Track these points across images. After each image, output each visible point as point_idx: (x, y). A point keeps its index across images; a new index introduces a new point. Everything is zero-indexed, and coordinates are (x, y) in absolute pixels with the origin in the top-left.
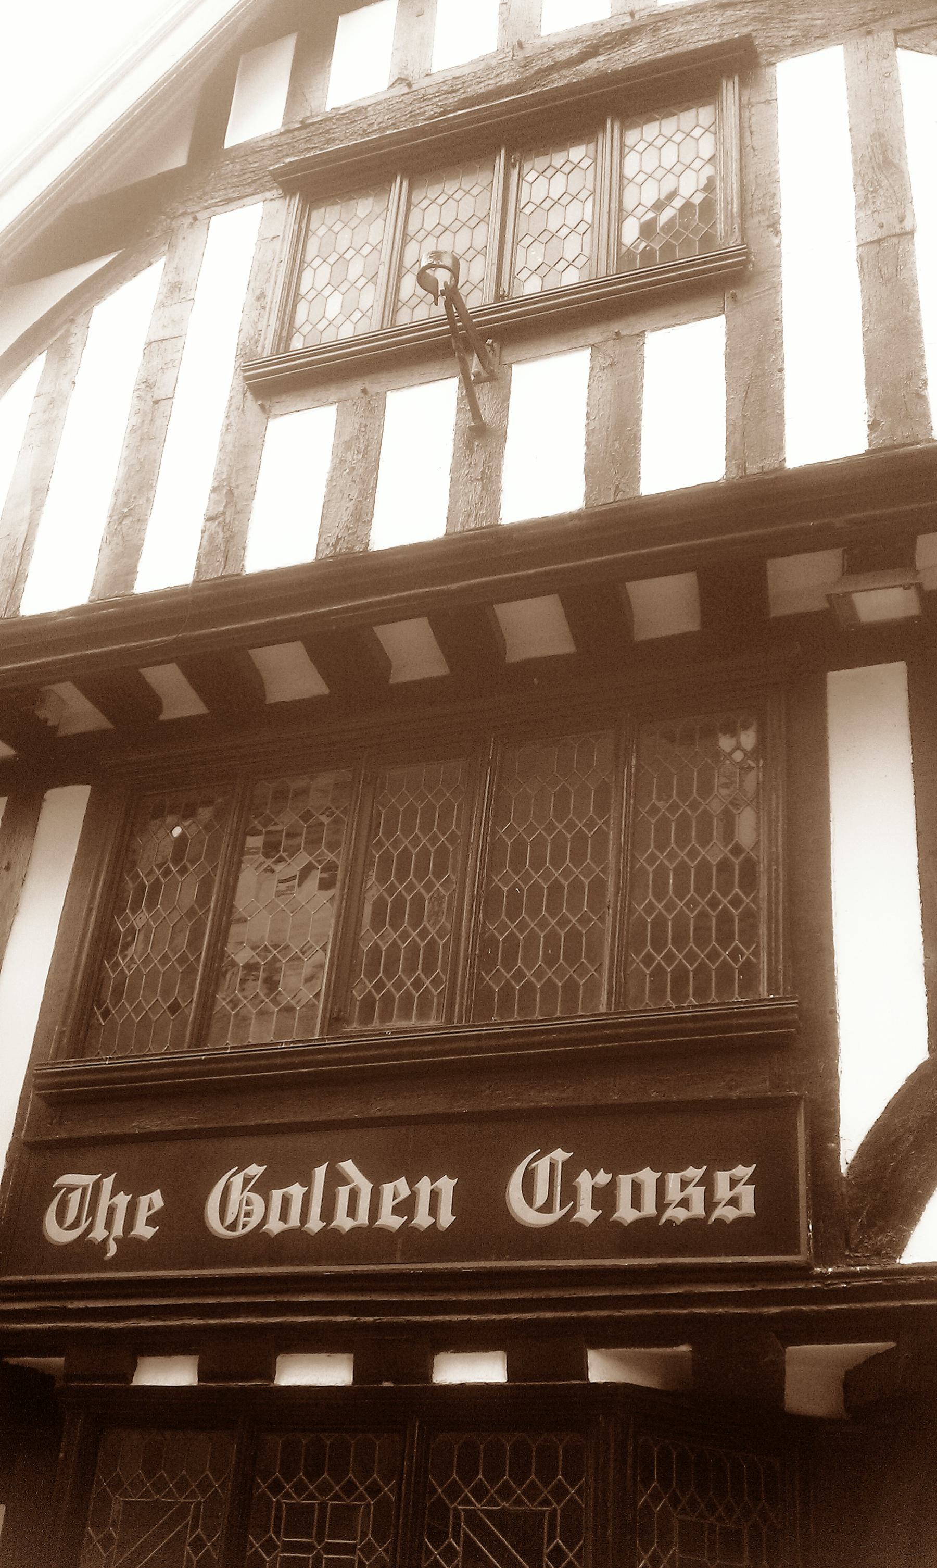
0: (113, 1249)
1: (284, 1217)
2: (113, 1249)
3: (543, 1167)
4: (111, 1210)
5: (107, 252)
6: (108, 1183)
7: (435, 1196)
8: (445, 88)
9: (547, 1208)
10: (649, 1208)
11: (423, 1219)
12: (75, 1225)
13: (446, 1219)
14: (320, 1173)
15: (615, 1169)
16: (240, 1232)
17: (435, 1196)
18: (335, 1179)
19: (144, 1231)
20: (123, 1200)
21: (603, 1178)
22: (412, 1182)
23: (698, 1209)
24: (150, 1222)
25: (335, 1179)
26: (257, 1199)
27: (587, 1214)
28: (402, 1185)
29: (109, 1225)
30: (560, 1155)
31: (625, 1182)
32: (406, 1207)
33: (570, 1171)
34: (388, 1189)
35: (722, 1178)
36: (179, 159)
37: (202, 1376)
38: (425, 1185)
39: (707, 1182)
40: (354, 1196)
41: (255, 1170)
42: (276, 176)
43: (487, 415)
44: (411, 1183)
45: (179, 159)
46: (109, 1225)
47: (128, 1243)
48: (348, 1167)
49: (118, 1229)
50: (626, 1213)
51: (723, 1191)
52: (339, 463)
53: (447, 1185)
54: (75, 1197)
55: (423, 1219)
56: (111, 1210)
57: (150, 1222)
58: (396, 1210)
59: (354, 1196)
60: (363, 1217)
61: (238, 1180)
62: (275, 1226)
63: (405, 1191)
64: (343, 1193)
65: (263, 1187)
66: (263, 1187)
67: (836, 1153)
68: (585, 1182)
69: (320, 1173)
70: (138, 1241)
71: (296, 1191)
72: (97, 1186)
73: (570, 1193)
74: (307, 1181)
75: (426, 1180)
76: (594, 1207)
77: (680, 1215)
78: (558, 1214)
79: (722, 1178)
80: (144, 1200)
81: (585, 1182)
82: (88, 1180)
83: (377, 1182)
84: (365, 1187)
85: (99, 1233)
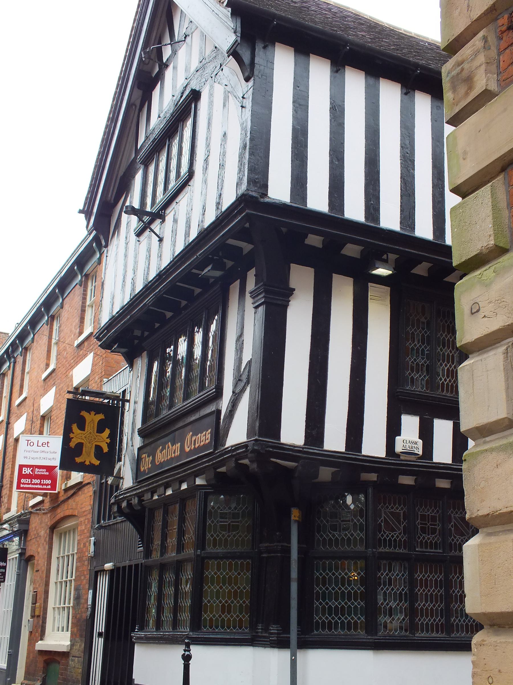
11: (176, 454)
13: (179, 453)
15: (196, 436)
20: (148, 458)
25: (168, 447)
26: (161, 454)
30: (191, 433)
31: (197, 437)
37: (158, 497)
38: (177, 446)
47: (148, 468)
50: (197, 446)
53: (179, 444)
55: (176, 454)
62: (162, 460)
74: (166, 449)
76: (194, 445)
78: (190, 448)
80: (150, 458)
81: (193, 439)
83: (172, 447)
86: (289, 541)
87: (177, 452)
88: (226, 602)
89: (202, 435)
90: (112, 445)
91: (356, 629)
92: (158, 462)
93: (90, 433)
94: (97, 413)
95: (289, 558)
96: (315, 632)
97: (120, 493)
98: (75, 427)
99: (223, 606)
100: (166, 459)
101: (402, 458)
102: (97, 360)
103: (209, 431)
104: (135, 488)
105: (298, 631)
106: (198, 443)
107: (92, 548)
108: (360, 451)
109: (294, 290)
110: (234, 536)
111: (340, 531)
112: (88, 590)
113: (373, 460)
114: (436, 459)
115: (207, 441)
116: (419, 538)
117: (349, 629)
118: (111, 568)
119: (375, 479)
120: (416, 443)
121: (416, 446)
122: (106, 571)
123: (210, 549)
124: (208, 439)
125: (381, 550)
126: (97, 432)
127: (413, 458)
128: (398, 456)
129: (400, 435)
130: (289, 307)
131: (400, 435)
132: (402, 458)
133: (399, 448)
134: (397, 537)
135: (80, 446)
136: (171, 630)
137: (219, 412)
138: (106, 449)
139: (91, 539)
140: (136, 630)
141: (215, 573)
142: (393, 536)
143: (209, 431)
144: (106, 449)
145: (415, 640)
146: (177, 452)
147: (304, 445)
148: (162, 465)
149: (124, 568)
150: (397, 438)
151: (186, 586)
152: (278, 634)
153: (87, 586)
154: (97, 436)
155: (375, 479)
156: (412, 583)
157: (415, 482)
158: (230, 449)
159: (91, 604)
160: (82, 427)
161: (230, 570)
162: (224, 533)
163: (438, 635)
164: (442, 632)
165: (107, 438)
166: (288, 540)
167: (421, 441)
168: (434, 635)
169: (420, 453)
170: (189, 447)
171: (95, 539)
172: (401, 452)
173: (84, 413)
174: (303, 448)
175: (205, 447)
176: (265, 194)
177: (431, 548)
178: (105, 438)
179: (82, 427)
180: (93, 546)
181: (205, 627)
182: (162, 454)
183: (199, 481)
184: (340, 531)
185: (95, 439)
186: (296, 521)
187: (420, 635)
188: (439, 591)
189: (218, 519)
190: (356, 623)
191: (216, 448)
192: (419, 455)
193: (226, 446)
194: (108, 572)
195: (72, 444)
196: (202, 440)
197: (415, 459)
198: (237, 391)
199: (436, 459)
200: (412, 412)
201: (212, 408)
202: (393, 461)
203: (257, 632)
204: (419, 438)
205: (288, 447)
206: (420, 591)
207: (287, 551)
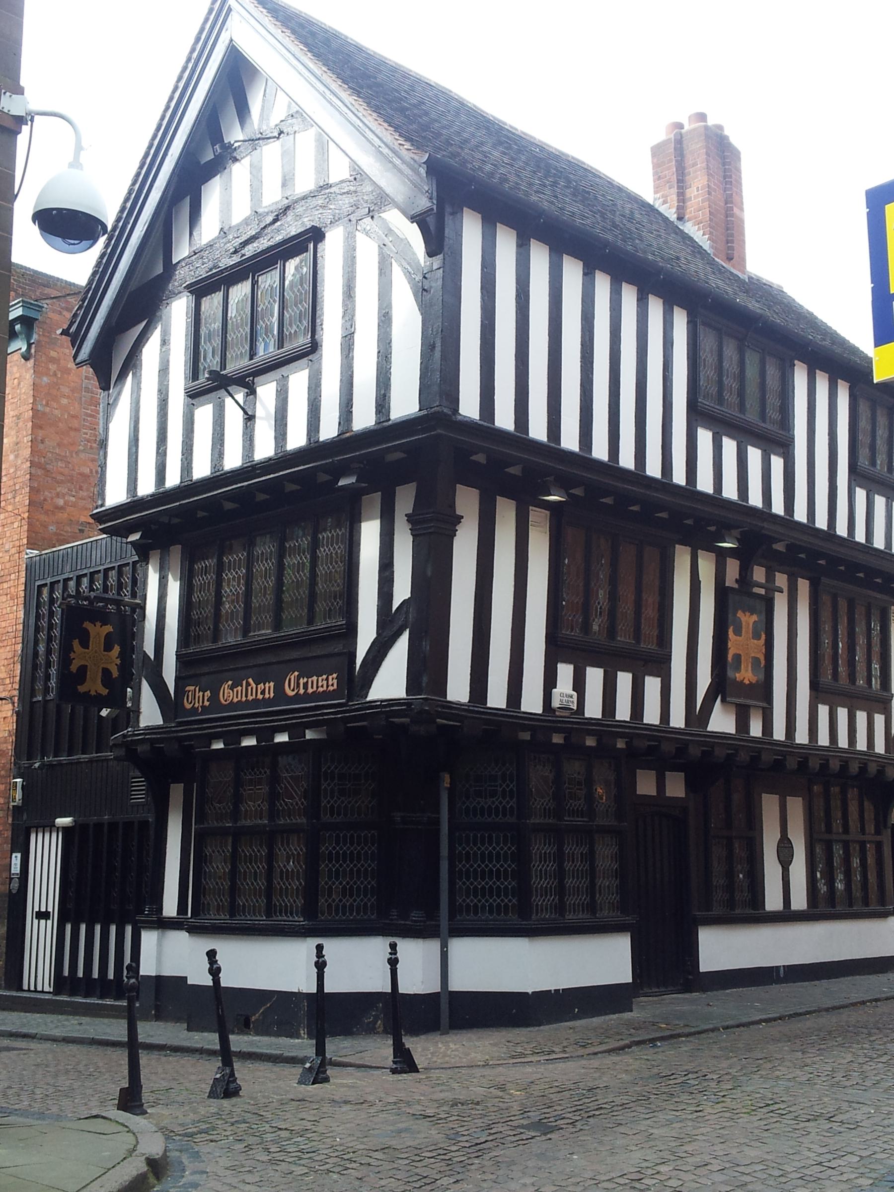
0: (200, 709)
1: (237, 697)
2: (200, 709)
3: (292, 677)
4: (199, 697)
5: (142, 321)
6: (197, 689)
7: (269, 688)
8: (235, 236)
9: (293, 690)
10: (315, 688)
11: (267, 696)
12: (191, 703)
13: (272, 695)
14: (244, 682)
15: (308, 678)
16: (228, 702)
17: (269, 688)
18: (248, 684)
19: (207, 703)
20: (201, 693)
21: (305, 680)
22: (264, 684)
23: (325, 688)
24: (208, 701)
25: (248, 684)
26: (231, 691)
27: (302, 691)
28: (262, 684)
29: (199, 702)
30: (296, 673)
31: (310, 680)
32: (263, 692)
33: (299, 678)
34: (259, 686)
35: (330, 677)
36: (159, 270)
38: (267, 685)
39: (327, 679)
40: (252, 689)
41: (230, 683)
42: (187, 287)
43: (250, 413)
44: (264, 684)
45: (159, 270)
46: (199, 702)
48: (250, 680)
49: (201, 704)
50: (310, 691)
51: (330, 683)
52: (214, 430)
53: (272, 684)
54: (190, 693)
55: (267, 696)
56: (199, 697)
57: (208, 701)
58: (261, 694)
59: (252, 689)
60: (254, 696)
61: (226, 686)
62: (235, 700)
63: (263, 688)
64: (250, 688)
65: (232, 688)
66: (232, 688)
67: (355, 667)
68: (302, 681)
69: (244, 682)
70: (205, 706)
71: (239, 688)
72: (195, 689)
73: (298, 685)
74: (242, 686)
75: (267, 684)
77: (321, 689)
78: (296, 691)
79: (330, 677)
80: (206, 694)
81: (302, 681)
82: (193, 687)
84: (254, 686)
85: (197, 705)
86: (438, 812)
87: (269, 693)
88: (348, 883)
89: (320, 679)
90: (121, 668)
91: (506, 913)
92: (226, 701)
93: (96, 652)
94: (104, 623)
95: (438, 832)
96: (458, 918)
97: (136, 732)
98: (76, 644)
99: (344, 888)
100: (244, 699)
101: (557, 713)
102: (5, 518)
103: (335, 675)
104: (173, 729)
105: (439, 917)
106: (312, 687)
107: (19, 795)
108: (520, 708)
109: (462, 517)
110: (356, 802)
111: (486, 798)
112: (9, 852)
113: (531, 716)
114: (587, 715)
115: (331, 688)
116: (567, 805)
117: (499, 914)
118: (71, 825)
119: (529, 738)
120: (571, 697)
121: (571, 699)
122: (58, 828)
123: (326, 818)
124: (332, 685)
125: (532, 821)
126: (104, 651)
127: (566, 713)
128: (554, 711)
129: (555, 688)
130: (455, 538)
131: (555, 688)
132: (557, 713)
133: (556, 703)
134: (547, 804)
135: (83, 669)
136: (264, 918)
137: (353, 655)
138: (115, 673)
139: (18, 780)
140: (146, 912)
141: (334, 848)
142: (543, 804)
143: (335, 675)
144: (115, 673)
145: (567, 923)
146: (269, 693)
147: (469, 702)
148: (232, 706)
149: (99, 826)
150: (554, 690)
151: (288, 862)
152: (425, 922)
153: (7, 847)
154: (104, 655)
155: (529, 738)
156: (560, 857)
157: (565, 740)
158: (379, 703)
159: (19, 872)
160: (85, 644)
161: (352, 844)
162: (343, 798)
163: (585, 916)
164: (587, 913)
165: (117, 658)
166: (437, 809)
167: (575, 694)
168: (580, 916)
169: (575, 708)
170: (293, 690)
171: (23, 781)
172: (559, 708)
173: (87, 625)
174: (469, 706)
175: (326, 695)
176: (456, 410)
177: (578, 816)
178: (114, 658)
179: (85, 644)
180: (21, 791)
181: (323, 915)
182: (233, 691)
183: (309, 735)
184: (486, 798)
185: (101, 659)
186: (447, 788)
187: (570, 917)
188: (584, 866)
189: (336, 781)
190: (506, 906)
191: (348, 701)
192: (573, 709)
193: (368, 699)
194: (60, 829)
195: (74, 668)
196: (320, 684)
197: (567, 714)
198: (388, 633)
199: (588, 714)
200: (566, 661)
201: (337, 647)
202: (550, 718)
203: (392, 920)
204: (574, 690)
205: (455, 706)
206: (568, 866)
207: (437, 822)
